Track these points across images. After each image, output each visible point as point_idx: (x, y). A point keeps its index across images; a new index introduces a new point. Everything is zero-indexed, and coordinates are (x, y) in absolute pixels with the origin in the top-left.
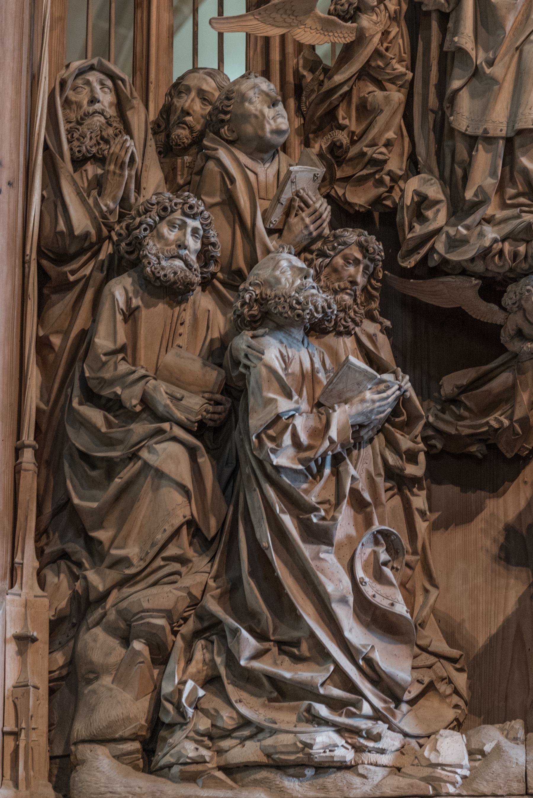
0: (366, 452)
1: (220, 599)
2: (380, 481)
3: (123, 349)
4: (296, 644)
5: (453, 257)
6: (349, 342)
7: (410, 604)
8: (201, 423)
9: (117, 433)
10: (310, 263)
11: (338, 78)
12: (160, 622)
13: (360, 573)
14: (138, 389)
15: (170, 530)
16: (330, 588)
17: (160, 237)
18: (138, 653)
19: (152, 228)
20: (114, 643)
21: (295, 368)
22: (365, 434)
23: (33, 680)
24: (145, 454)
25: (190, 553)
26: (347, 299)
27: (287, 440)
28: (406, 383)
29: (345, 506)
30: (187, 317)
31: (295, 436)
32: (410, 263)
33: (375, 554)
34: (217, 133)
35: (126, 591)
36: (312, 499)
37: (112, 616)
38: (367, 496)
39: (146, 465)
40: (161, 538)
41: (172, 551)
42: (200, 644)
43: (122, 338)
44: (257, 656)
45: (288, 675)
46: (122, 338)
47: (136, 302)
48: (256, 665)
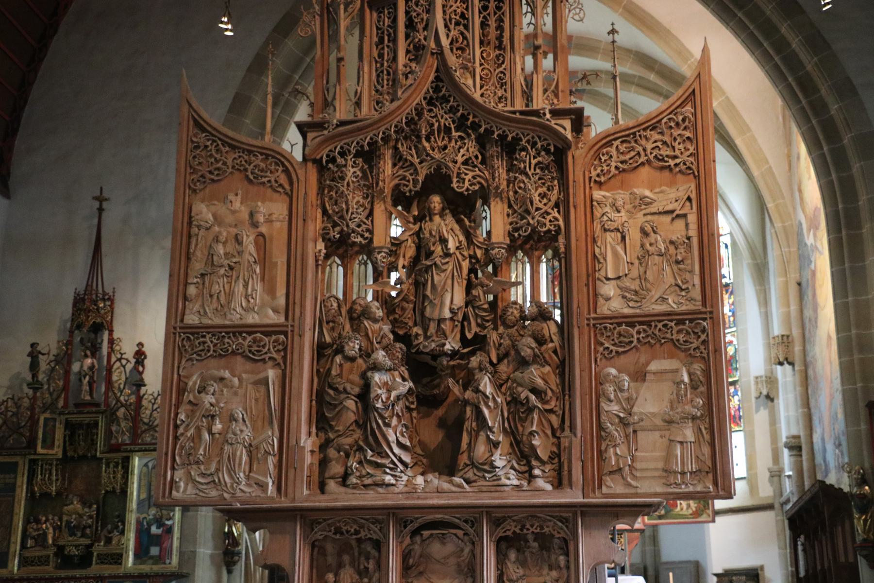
0: (401, 402)
1: (363, 441)
2: (404, 410)
3: (338, 375)
4: (382, 453)
5: (424, 350)
6: (396, 373)
7: (411, 442)
8: (359, 395)
9: (336, 397)
10: (387, 353)
11: (396, 301)
12: (347, 447)
13: (398, 435)
14: (342, 386)
15: (350, 422)
16: (390, 439)
17: (348, 345)
18: (341, 456)
19: (347, 343)
20: (336, 452)
21: (382, 381)
22: (401, 397)
23: (314, 462)
24: (344, 403)
25: (356, 428)
26: (397, 361)
27: (380, 400)
28: (411, 384)
29: (395, 418)
30: (356, 366)
31: (382, 400)
32: (414, 351)
33: (402, 430)
34: (364, 316)
35: (339, 439)
36: (386, 415)
37: (335, 445)
38: (400, 414)
39: (344, 406)
40: (348, 425)
41: (351, 428)
42: (357, 453)
43: (339, 372)
44: (372, 456)
45: (379, 461)
46: (339, 372)
47: (342, 362)
48: (372, 459)
